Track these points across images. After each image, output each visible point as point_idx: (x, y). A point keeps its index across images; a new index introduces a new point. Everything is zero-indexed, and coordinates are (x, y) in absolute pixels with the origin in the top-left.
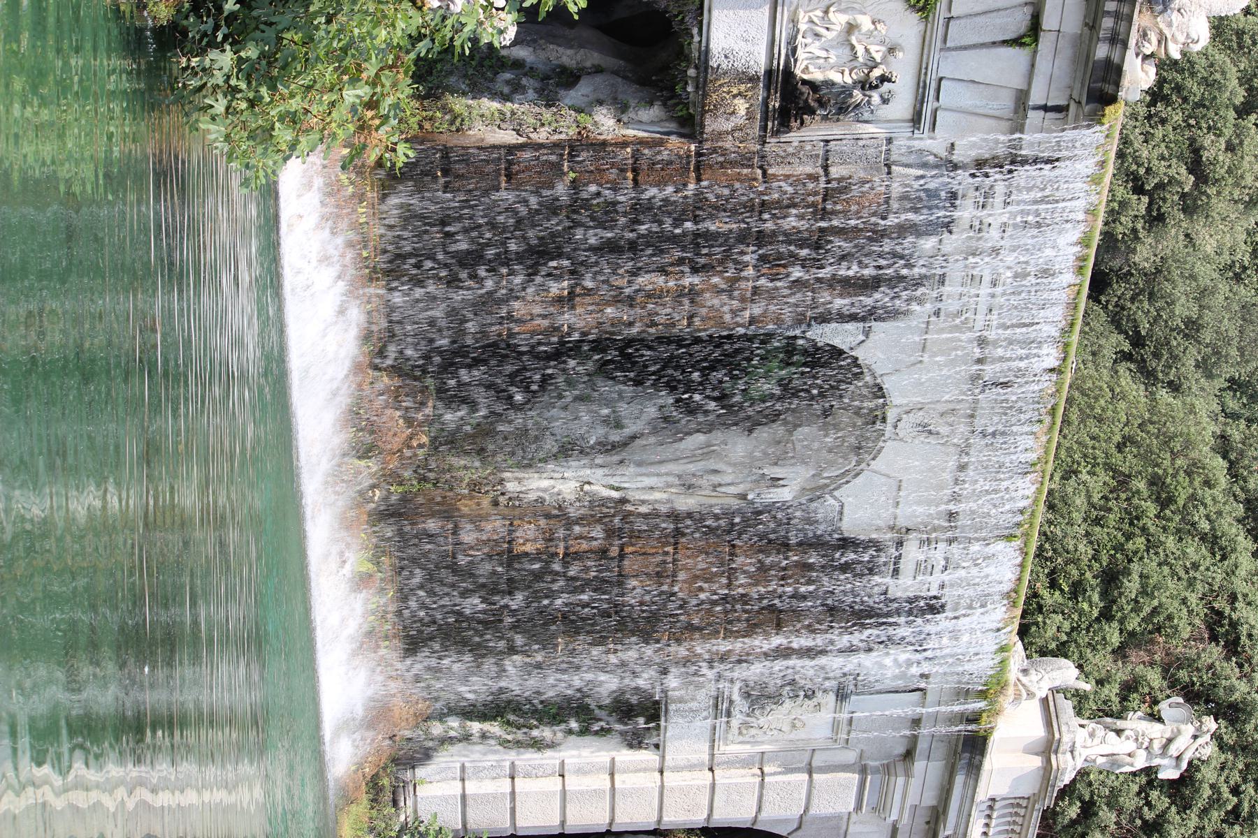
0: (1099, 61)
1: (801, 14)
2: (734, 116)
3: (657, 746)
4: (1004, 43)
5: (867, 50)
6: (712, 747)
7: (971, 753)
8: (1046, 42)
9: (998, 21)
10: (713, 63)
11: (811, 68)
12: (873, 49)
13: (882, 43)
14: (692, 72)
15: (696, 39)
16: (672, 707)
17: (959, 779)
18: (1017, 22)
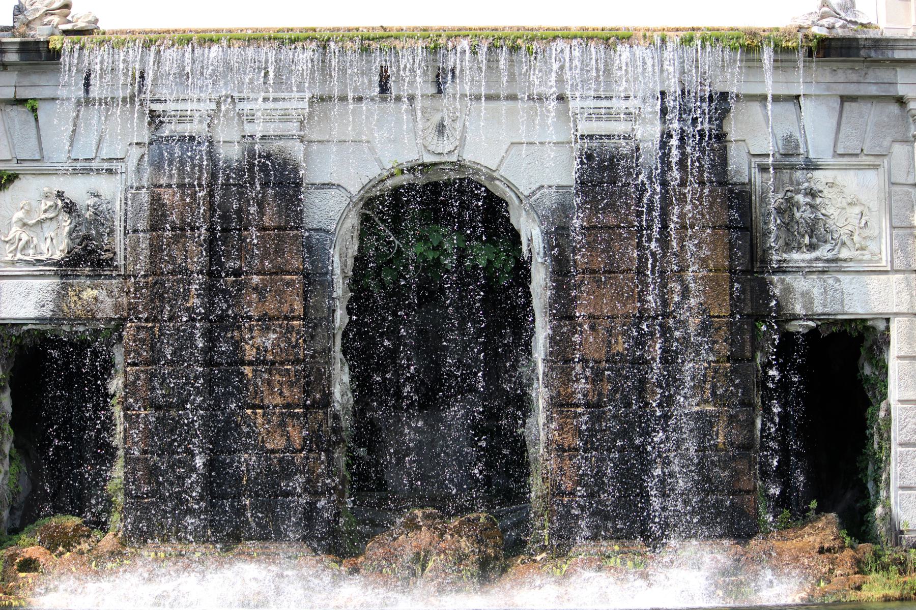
0: (22, 59)
1: (7, 259)
2: (99, 297)
3: (888, 320)
4: (36, 120)
5: (45, 211)
6: (886, 272)
7: (858, 49)
8: (23, 94)
9: (17, 127)
10: (49, 314)
11: (61, 248)
12: (43, 207)
13: (40, 201)
14: (66, 328)
15: (30, 327)
16: (819, 309)
17: (899, 55)
18: (18, 115)
